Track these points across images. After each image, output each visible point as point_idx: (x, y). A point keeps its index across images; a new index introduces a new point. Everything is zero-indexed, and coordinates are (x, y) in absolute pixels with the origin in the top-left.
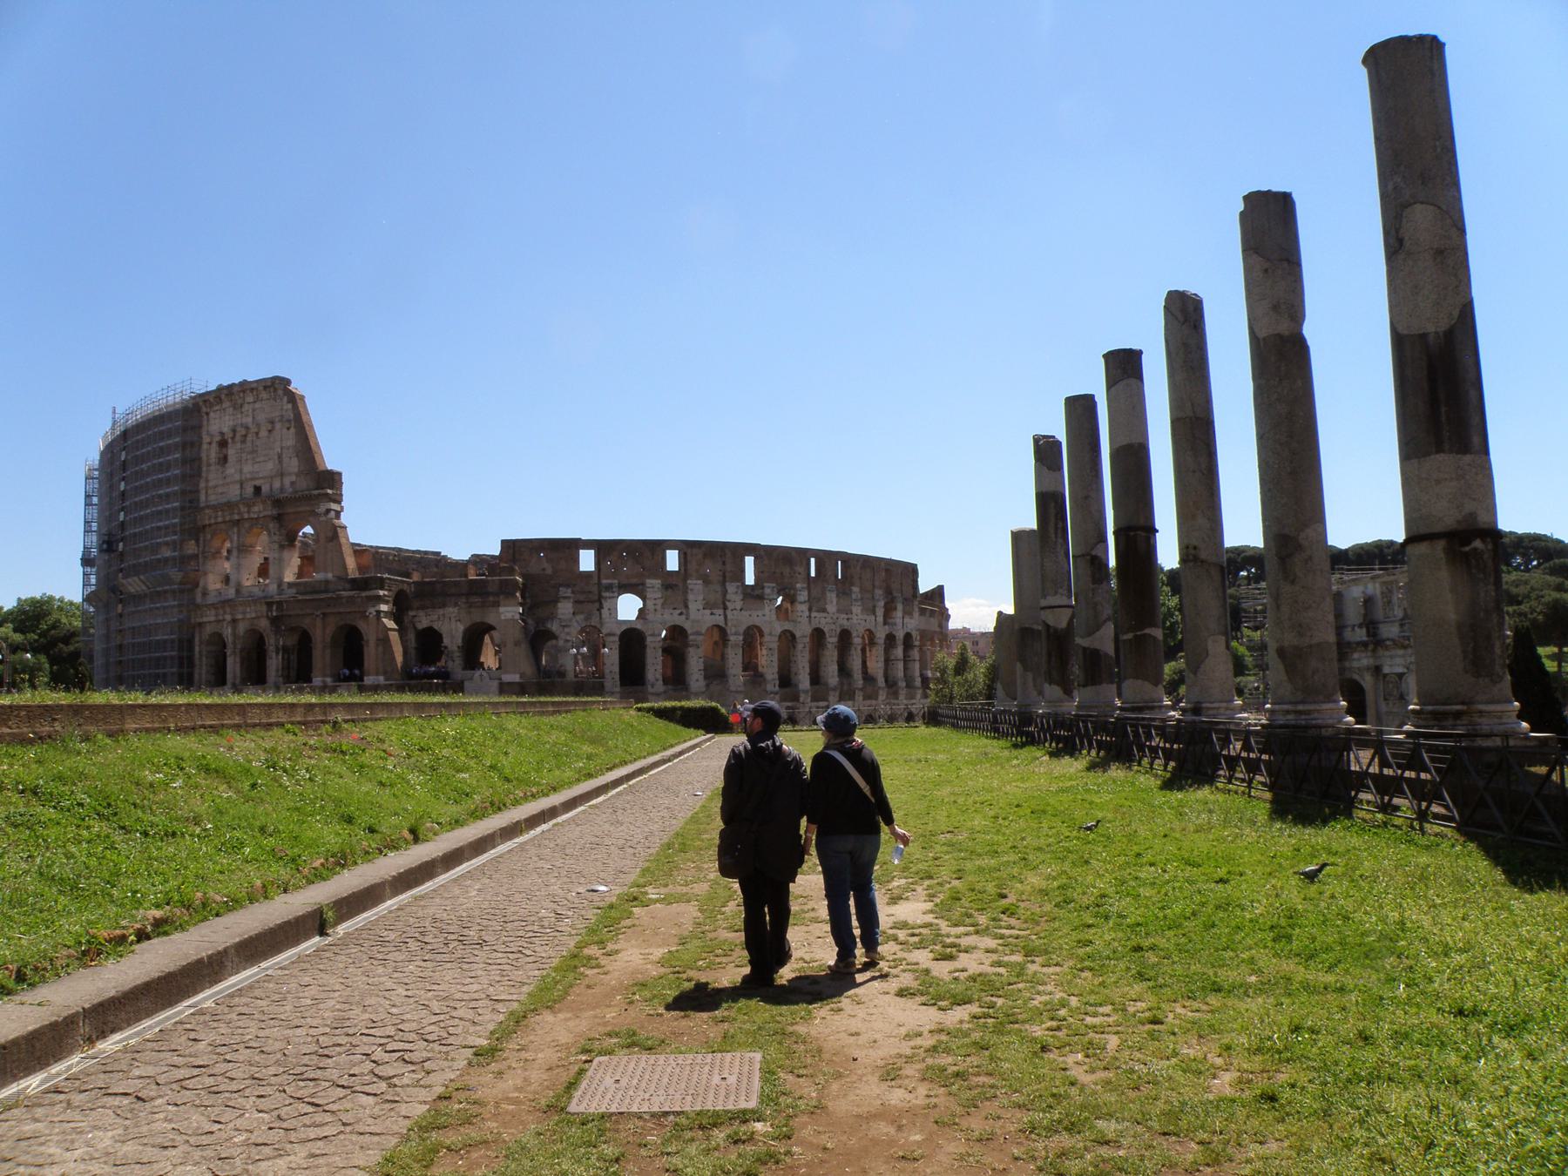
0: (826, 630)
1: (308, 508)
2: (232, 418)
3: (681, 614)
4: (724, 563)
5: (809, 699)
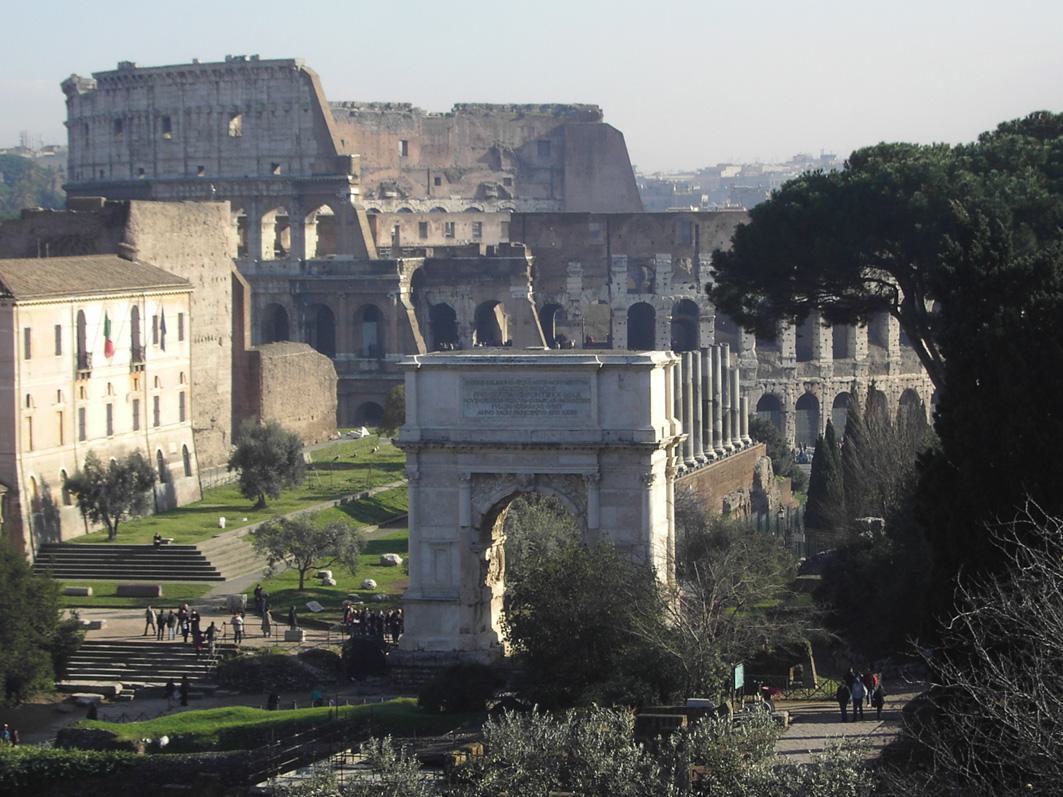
3: (692, 288)
5: (831, 374)
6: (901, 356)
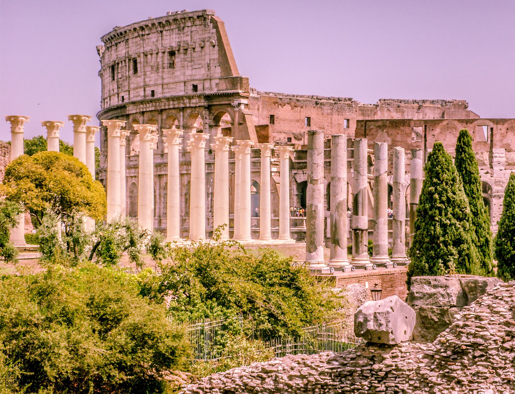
1: (227, 102)
2: (177, 36)
3: (487, 173)
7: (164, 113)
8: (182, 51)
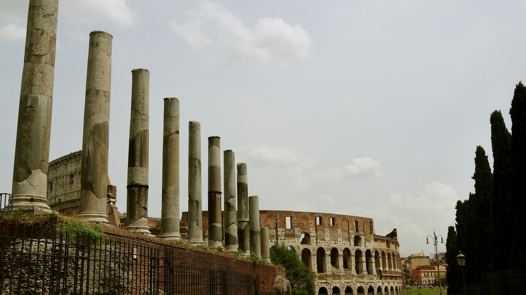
0: (325, 248)
4: (276, 220)
6: (345, 273)
7: (65, 211)
8: (77, 173)
